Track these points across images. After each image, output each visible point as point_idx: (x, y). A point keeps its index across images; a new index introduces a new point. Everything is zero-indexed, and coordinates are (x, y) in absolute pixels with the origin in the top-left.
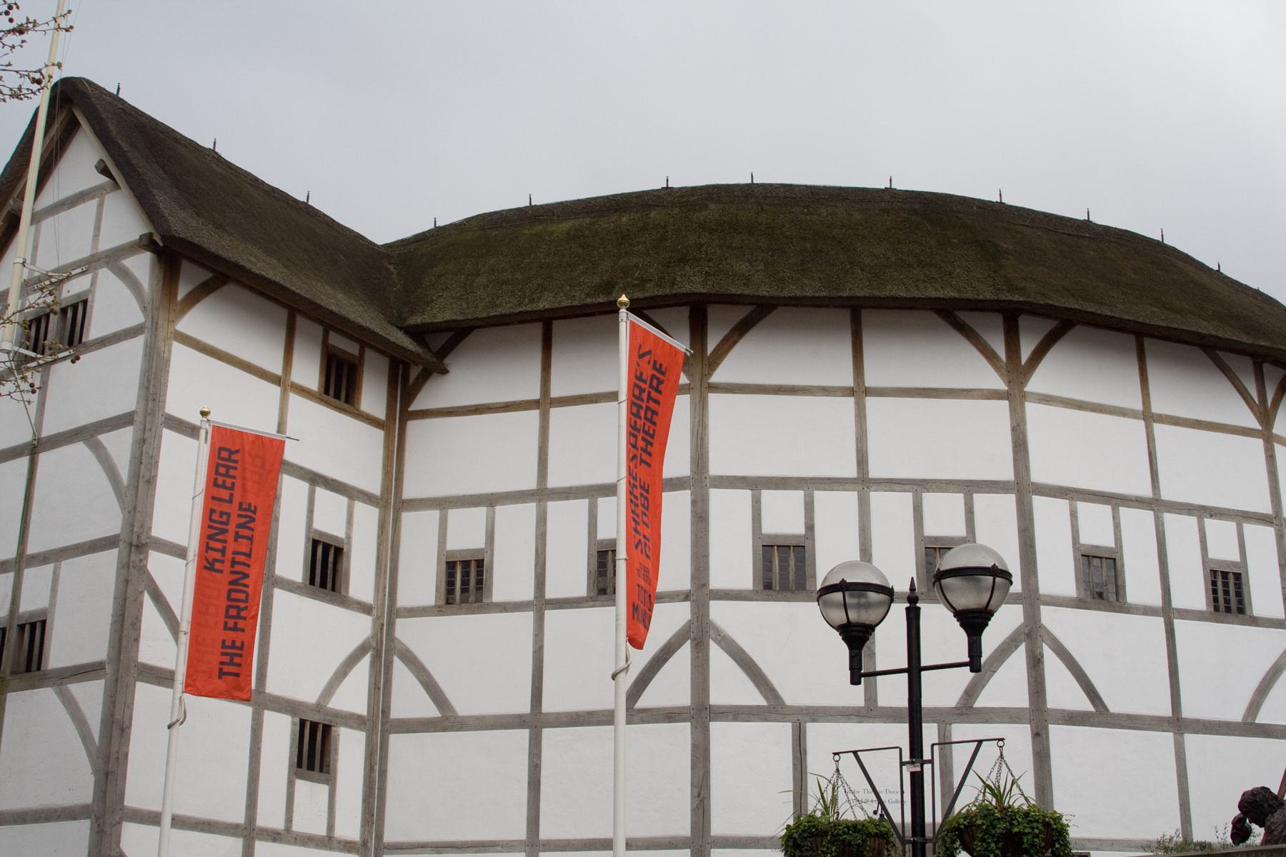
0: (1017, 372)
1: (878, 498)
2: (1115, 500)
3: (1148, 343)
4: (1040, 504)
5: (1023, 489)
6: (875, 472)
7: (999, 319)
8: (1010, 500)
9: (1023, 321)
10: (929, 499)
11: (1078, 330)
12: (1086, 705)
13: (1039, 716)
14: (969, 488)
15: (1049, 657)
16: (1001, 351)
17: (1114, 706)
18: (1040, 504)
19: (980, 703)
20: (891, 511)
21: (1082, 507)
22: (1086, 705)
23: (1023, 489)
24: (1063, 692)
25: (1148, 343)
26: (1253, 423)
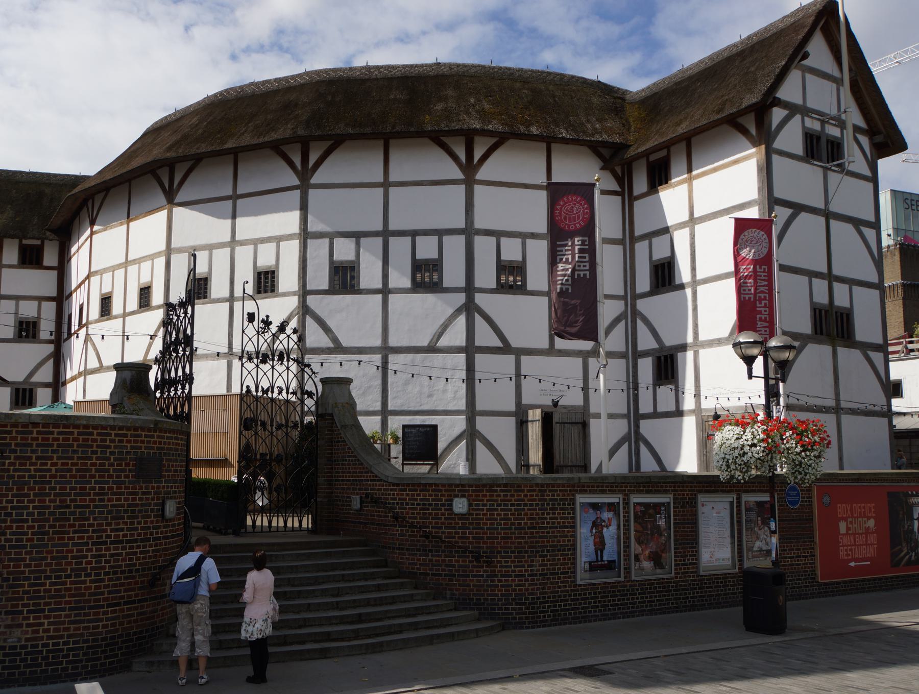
0: (470, 168)
1: (392, 240)
2: (524, 236)
3: (554, 146)
4: (478, 240)
5: (469, 232)
6: (392, 227)
7: (463, 139)
8: (462, 239)
9: (477, 139)
10: (419, 239)
11: (511, 141)
12: (498, 343)
13: (470, 350)
14: (440, 233)
15: (478, 318)
16: (463, 157)
17: (515, 343)
18: (478, 240)
19: (443, 342)
20: (400, 247)
21: (504, 240)
22: (498, 343)
23: (469, 232)
24: (485, 336)
25: (554, 146)
26: (617, 188)
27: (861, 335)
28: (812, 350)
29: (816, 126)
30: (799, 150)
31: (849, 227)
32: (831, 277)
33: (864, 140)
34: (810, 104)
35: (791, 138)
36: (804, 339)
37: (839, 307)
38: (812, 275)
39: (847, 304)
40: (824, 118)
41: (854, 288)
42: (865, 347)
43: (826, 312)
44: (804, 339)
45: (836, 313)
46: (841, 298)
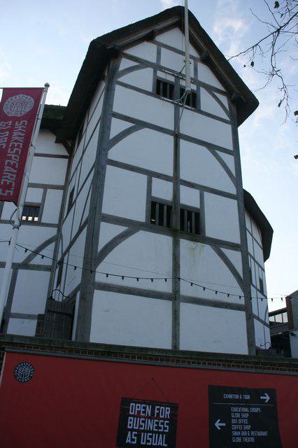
27: (211, 231)
28: (142, 236)
29: (171, 79)
30: (150, 89)
31: (204, 149)
32: (176, 180)
33: (224, 99)
34: (163, 63)
35: (145, 79)
36: (132, 227)
37: (182, 205)
38: (151, 175)
39: (196, 204)
40: (179, 76)
41: (206, 194)
42: (217, 244)
43: (169, 208)
44: (132, 227)
45: (182, 211)
46: (189, 198)
